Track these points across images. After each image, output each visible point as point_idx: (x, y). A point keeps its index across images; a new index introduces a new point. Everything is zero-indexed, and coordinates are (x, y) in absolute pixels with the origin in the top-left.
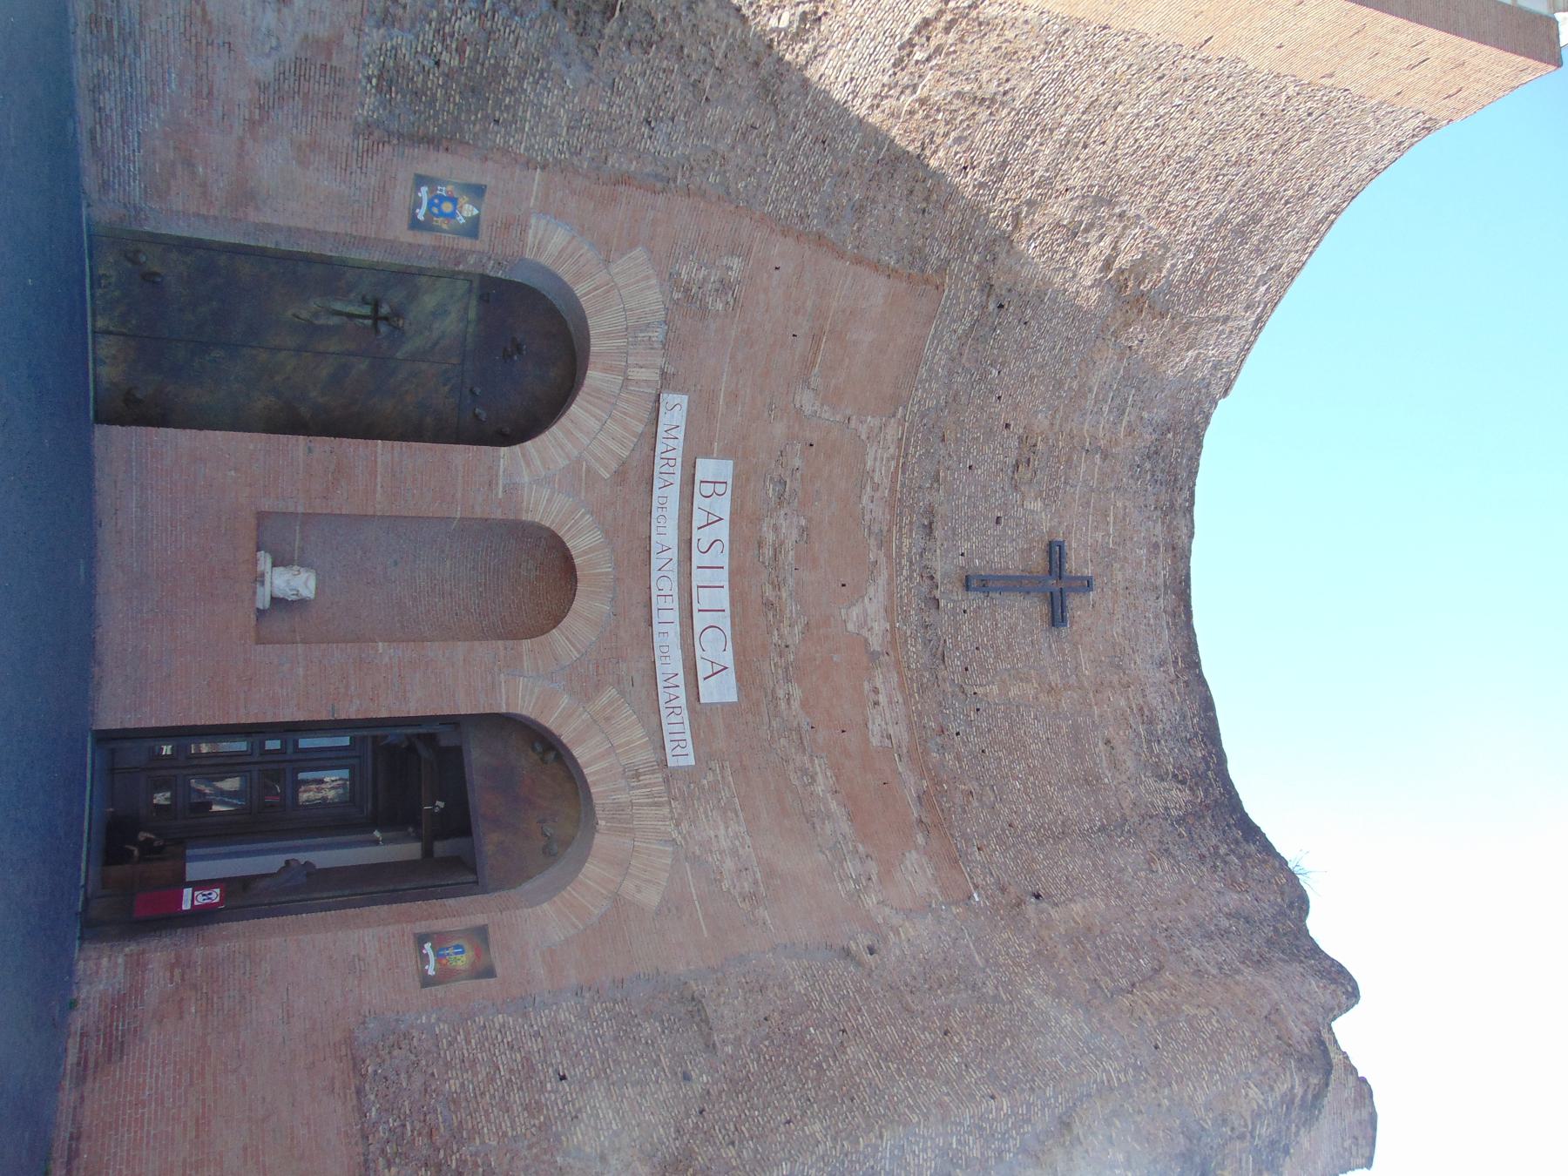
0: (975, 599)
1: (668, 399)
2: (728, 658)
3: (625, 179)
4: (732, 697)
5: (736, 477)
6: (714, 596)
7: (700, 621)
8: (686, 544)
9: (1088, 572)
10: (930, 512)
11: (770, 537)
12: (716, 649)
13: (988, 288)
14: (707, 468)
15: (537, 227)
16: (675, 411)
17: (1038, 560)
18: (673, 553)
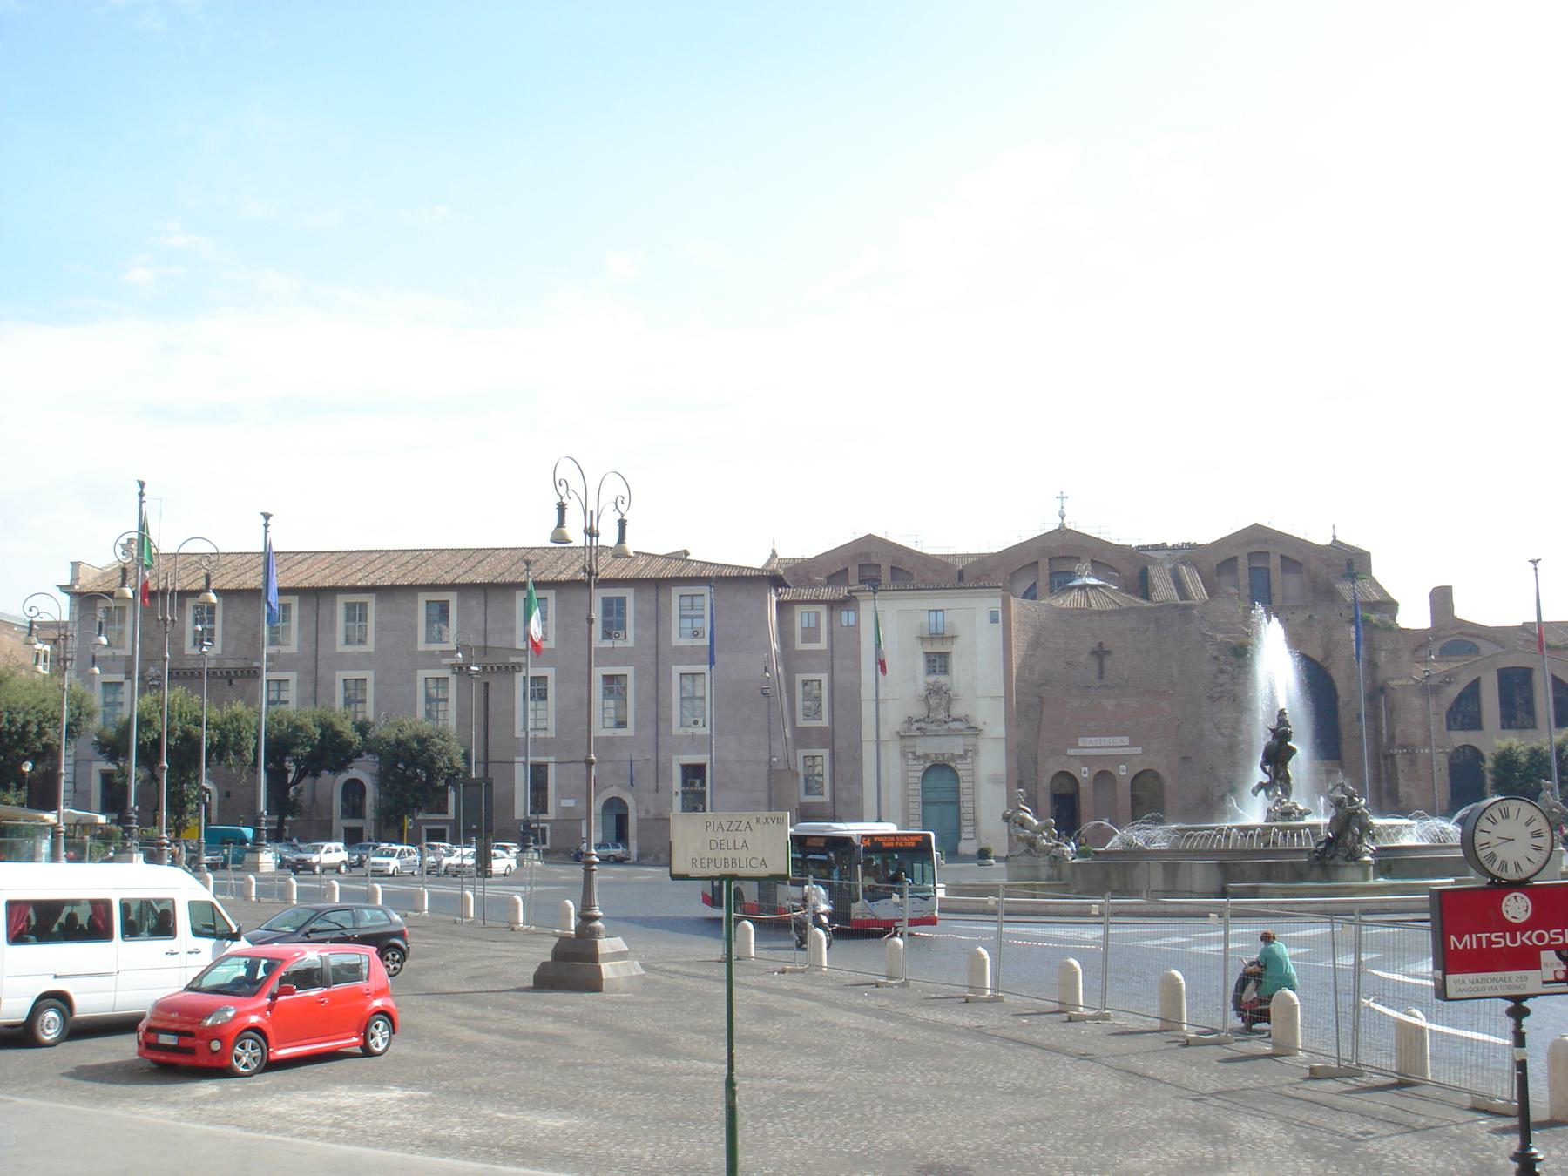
0: (1105, 675)
1: (1068, 753)
2: (1119, 738)
3: (1036, 770)
4: (1127, 738)
5: (1081, 737)
6: (1107, 741)
7: (1111, 744)
8: (1096, 747)
9: (1098, 641)
10: (1085, 687)
11: (1094, 728)
12: (1117, 741)
13: (1040, 685)
14: (1080, 744)
15: (1045, 784)
16: (1071, 752)
17: (1094, 657)
18: (1098, 750)
